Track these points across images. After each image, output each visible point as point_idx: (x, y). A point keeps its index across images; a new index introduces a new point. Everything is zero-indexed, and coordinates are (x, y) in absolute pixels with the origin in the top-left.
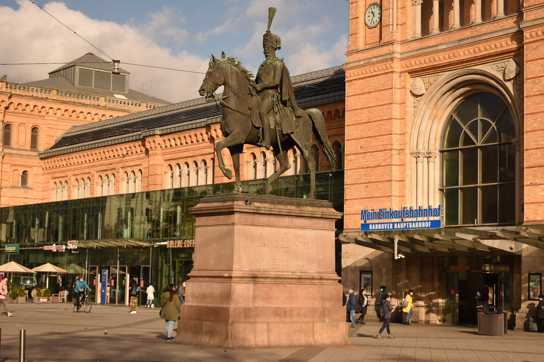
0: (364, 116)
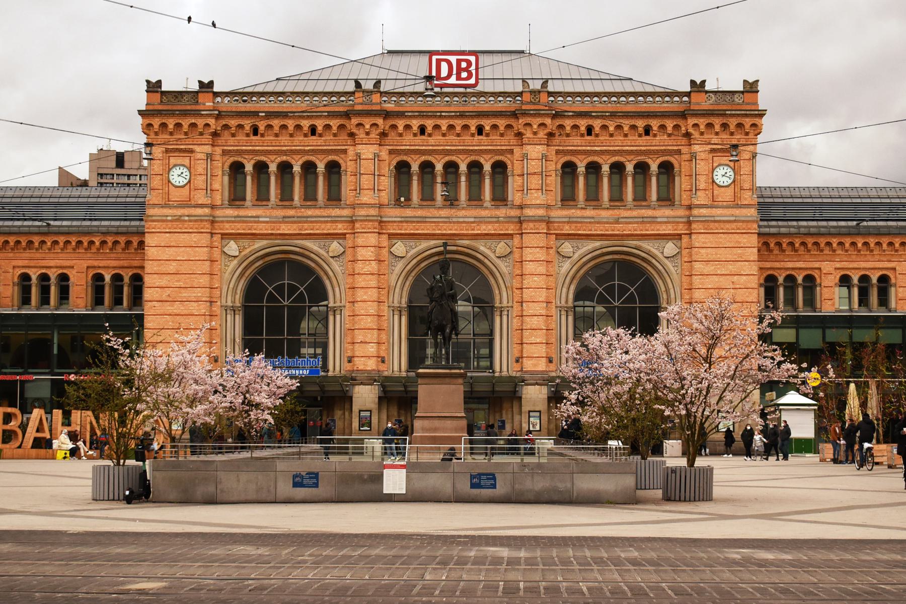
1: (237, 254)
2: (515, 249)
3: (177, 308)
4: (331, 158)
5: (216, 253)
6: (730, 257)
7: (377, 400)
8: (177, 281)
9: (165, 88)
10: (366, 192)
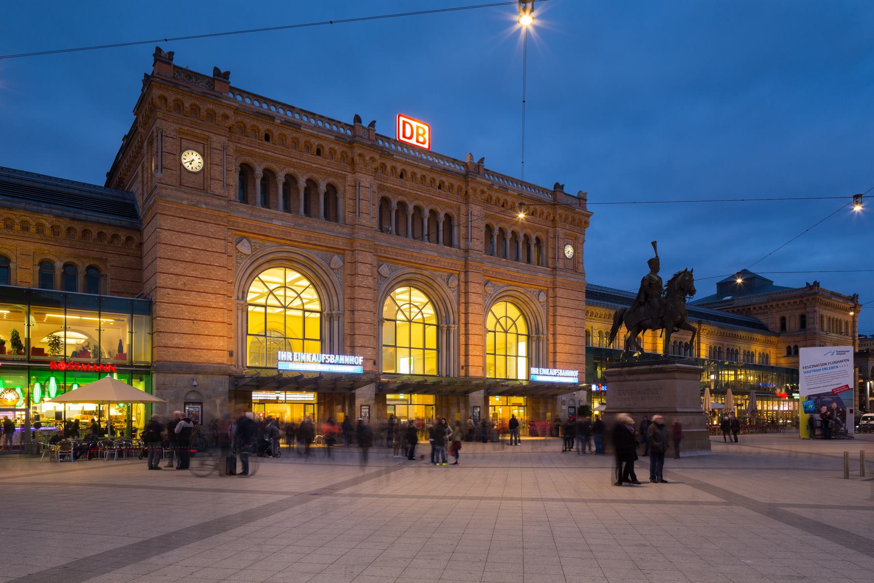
0: (187, 255)
5: (231, 249)
9: (176, 61)
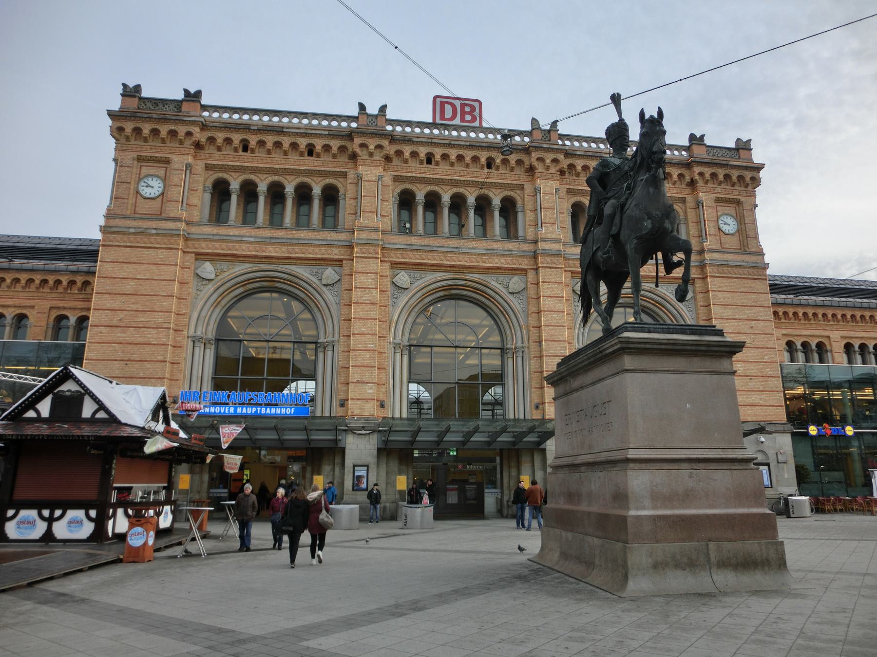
0: (128, 287)
1: (213, 276)
2: (529, 285)
3: (131, 335)
4: (328, 181)
6: (746, 302)
7: (375, 452)
8: (133, 303)
9: (145, 94)
10: (368, 214)
